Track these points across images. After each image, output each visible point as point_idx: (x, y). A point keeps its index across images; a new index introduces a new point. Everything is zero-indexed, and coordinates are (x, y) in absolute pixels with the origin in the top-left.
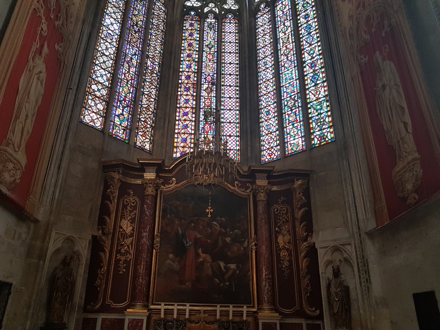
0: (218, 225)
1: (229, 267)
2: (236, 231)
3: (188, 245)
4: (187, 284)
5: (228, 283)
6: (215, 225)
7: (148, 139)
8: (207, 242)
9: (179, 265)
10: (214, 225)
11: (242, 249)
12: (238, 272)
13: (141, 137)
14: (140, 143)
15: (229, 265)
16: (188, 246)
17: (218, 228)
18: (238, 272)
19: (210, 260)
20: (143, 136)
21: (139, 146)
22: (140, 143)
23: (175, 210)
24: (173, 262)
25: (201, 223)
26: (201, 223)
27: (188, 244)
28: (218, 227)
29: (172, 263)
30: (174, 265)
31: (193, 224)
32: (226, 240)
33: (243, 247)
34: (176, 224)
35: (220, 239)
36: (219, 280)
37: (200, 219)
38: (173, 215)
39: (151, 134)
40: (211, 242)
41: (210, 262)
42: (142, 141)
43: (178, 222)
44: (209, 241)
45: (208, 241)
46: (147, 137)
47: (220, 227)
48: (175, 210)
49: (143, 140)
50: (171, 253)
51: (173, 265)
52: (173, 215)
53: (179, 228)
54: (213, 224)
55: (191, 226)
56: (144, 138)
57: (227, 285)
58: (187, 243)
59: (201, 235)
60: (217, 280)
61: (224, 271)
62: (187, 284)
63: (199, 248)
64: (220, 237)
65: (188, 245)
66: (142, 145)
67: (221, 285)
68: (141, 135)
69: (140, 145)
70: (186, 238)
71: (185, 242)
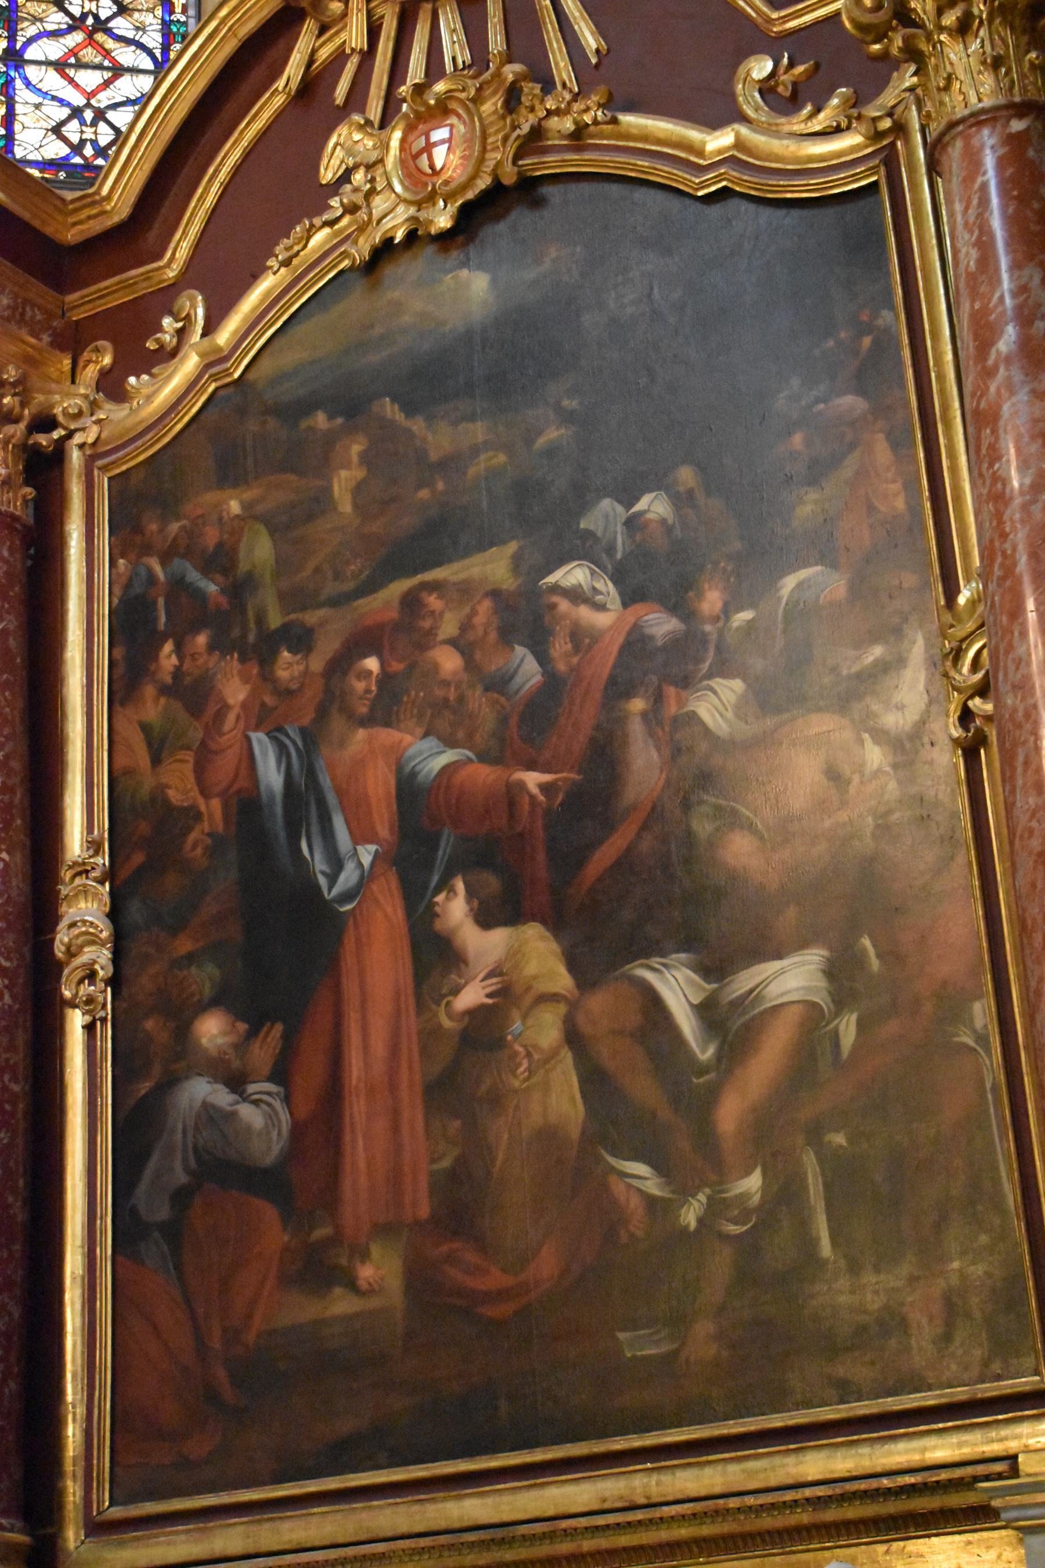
0: (607, 587)
1: (753, 996)
2: (789, 583)
3: (348, 877)
4: (366, 1273)
5: (753, 1183)
6: (576, 595)
7: (135, 71)
8: (513, 793)
9: (287, 1100)
10: (564, 605)
11: (875, 755)
12: (848, 1029)
13: (52, 80)
14: (57, 130)
15: (744, 981)
16: (347, 896)
17: (602, 620)
18: (848, 1029)
19: (563, 981)
20: (80, 65)
21: (46, 165)
22: (57, 130)
23: (212, 588)
24: (236, 1083)
25: (449, 627)
26: (449, 627)
27: (350, 867)
28: (601, 607)
29: (222, 1097)
30: (251, 1115)
31: (372, 664)
32: (693, 716)
33: (880, 736)
34: (231, 717)
35: (636, 728)
36: (660, 1167)
37: (435, 587)
38: (202, 640)
39: (166, 25)
40: (544, 788)
41: (554, 998)
42: (76, 113)
43: (241, 696)
44: (533, 779)
45: (522, 785)
46: (126, 56)
47: (631, 597)
48: (212, 588)
49: (79, 100)
50: (216, 1002)
51: (234, 1114)
52: (202, 640)
53: (259, 739)
54: (555, 589)
55: (360, 686)
56: (90, 79)
57: (745, 1196)
58: (337, 865)
59: (451, 743)
60: (640, 1169)
61: (706, 1054)
62: (366, 1273)
63: (445, 884)
64: (638, 705)
65: (348, 877)
66: (77, 149)
67: (690, 1216)
68: (59, 66)
69: (56, 150)
70: (325, 820)
71: (320, 864)
